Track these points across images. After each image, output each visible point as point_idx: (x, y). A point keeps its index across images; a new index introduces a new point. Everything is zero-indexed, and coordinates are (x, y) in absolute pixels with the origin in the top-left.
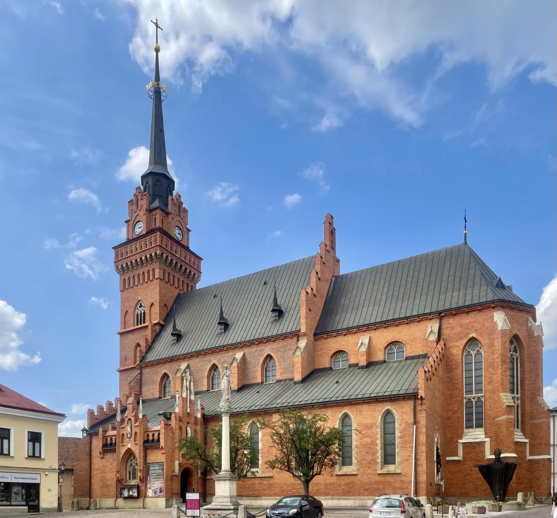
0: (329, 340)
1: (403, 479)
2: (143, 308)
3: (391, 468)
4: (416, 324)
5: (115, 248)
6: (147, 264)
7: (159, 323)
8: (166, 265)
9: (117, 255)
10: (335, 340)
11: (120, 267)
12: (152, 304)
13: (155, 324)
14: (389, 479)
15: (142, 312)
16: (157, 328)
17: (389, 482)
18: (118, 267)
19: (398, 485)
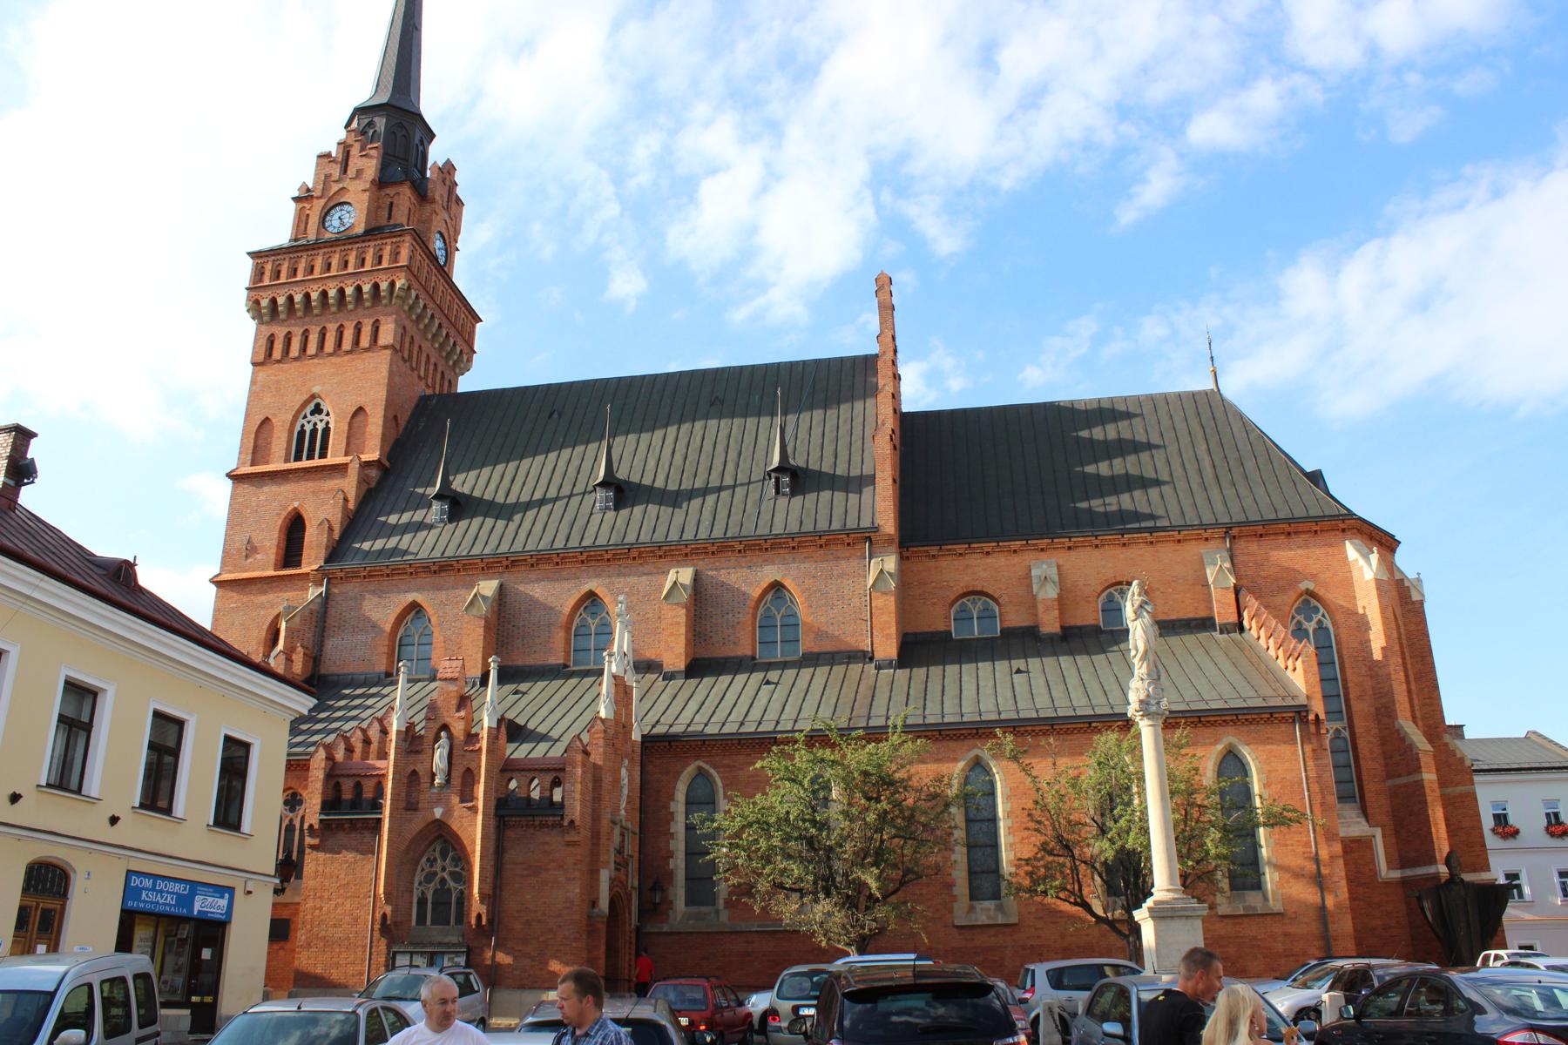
0: (944, 563)
1: (1292, 929)
2: (322, 416)
3: (1253, 898)
4: (1171, 547)
5: (255, 255)
6: (339, 310)
7: (379, 461)
8: (409, 317)
9: (258, 273)
10: (959, 563)
11: (264, 303)
12: (360, 409)
13: (368, 464)
14: (1252, 929)
15: (320, 426)
16: (374, 473)
17: (1254, 938)
18: (257, 302)
19: (1280, 947)
